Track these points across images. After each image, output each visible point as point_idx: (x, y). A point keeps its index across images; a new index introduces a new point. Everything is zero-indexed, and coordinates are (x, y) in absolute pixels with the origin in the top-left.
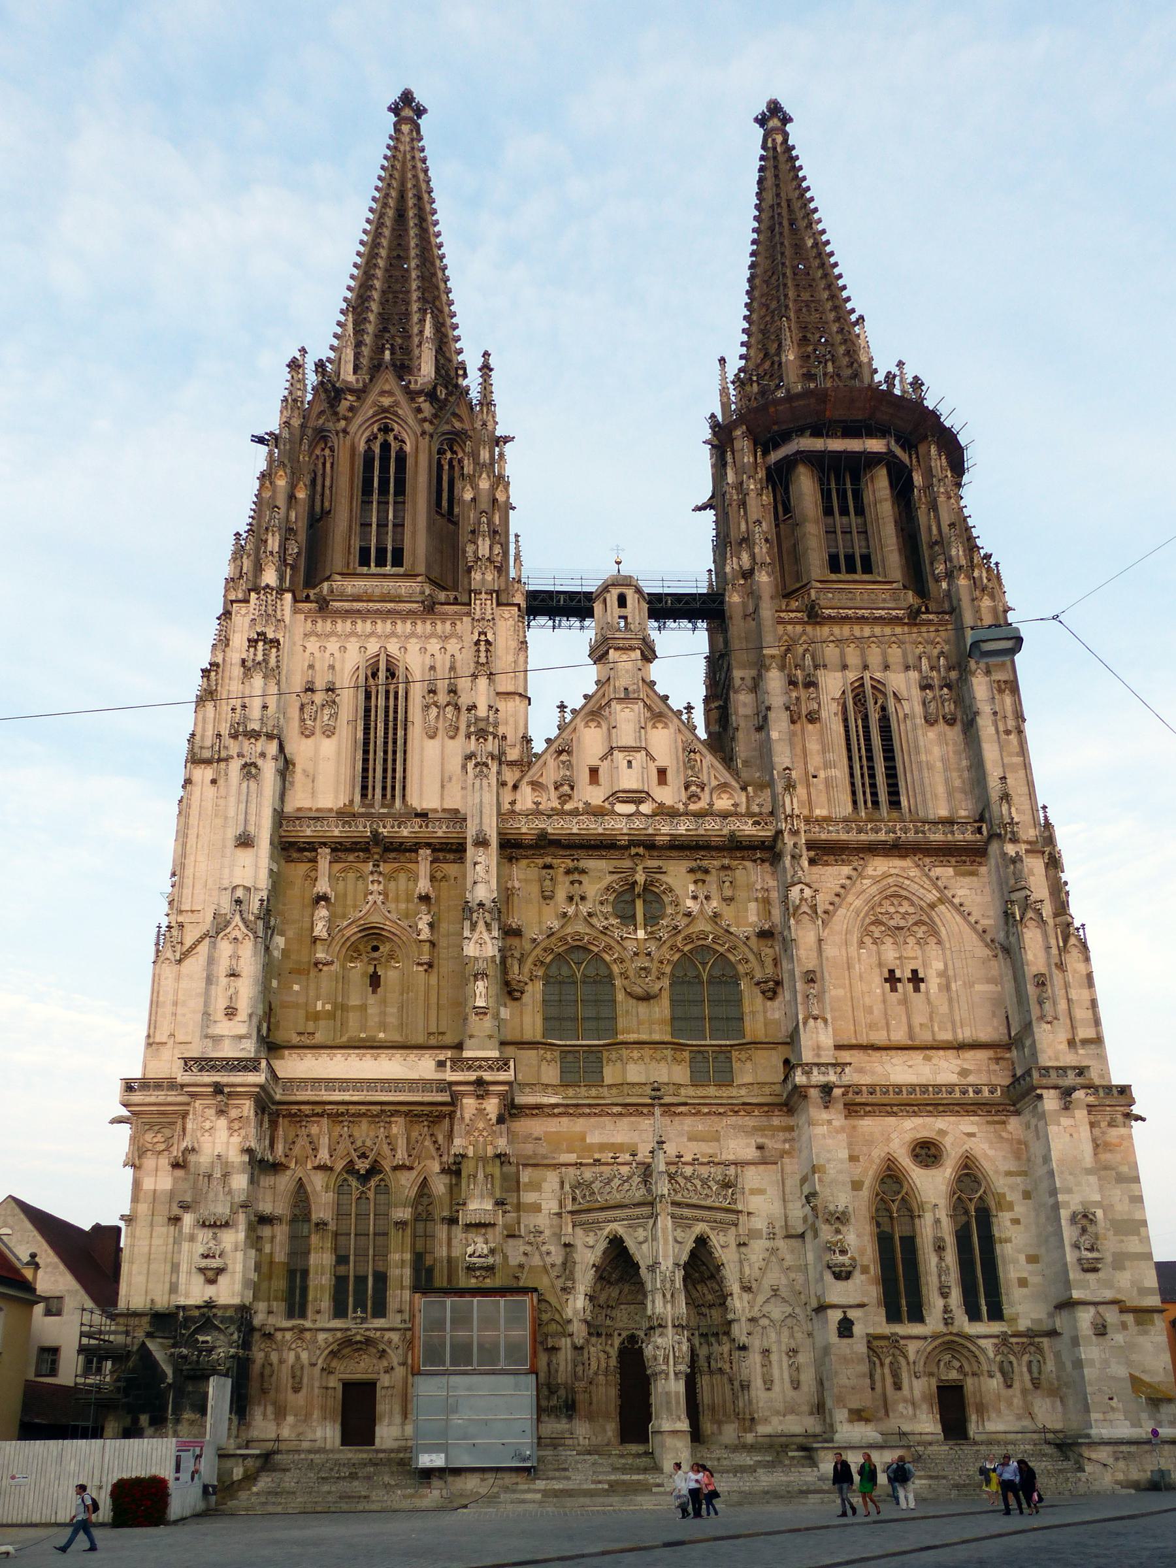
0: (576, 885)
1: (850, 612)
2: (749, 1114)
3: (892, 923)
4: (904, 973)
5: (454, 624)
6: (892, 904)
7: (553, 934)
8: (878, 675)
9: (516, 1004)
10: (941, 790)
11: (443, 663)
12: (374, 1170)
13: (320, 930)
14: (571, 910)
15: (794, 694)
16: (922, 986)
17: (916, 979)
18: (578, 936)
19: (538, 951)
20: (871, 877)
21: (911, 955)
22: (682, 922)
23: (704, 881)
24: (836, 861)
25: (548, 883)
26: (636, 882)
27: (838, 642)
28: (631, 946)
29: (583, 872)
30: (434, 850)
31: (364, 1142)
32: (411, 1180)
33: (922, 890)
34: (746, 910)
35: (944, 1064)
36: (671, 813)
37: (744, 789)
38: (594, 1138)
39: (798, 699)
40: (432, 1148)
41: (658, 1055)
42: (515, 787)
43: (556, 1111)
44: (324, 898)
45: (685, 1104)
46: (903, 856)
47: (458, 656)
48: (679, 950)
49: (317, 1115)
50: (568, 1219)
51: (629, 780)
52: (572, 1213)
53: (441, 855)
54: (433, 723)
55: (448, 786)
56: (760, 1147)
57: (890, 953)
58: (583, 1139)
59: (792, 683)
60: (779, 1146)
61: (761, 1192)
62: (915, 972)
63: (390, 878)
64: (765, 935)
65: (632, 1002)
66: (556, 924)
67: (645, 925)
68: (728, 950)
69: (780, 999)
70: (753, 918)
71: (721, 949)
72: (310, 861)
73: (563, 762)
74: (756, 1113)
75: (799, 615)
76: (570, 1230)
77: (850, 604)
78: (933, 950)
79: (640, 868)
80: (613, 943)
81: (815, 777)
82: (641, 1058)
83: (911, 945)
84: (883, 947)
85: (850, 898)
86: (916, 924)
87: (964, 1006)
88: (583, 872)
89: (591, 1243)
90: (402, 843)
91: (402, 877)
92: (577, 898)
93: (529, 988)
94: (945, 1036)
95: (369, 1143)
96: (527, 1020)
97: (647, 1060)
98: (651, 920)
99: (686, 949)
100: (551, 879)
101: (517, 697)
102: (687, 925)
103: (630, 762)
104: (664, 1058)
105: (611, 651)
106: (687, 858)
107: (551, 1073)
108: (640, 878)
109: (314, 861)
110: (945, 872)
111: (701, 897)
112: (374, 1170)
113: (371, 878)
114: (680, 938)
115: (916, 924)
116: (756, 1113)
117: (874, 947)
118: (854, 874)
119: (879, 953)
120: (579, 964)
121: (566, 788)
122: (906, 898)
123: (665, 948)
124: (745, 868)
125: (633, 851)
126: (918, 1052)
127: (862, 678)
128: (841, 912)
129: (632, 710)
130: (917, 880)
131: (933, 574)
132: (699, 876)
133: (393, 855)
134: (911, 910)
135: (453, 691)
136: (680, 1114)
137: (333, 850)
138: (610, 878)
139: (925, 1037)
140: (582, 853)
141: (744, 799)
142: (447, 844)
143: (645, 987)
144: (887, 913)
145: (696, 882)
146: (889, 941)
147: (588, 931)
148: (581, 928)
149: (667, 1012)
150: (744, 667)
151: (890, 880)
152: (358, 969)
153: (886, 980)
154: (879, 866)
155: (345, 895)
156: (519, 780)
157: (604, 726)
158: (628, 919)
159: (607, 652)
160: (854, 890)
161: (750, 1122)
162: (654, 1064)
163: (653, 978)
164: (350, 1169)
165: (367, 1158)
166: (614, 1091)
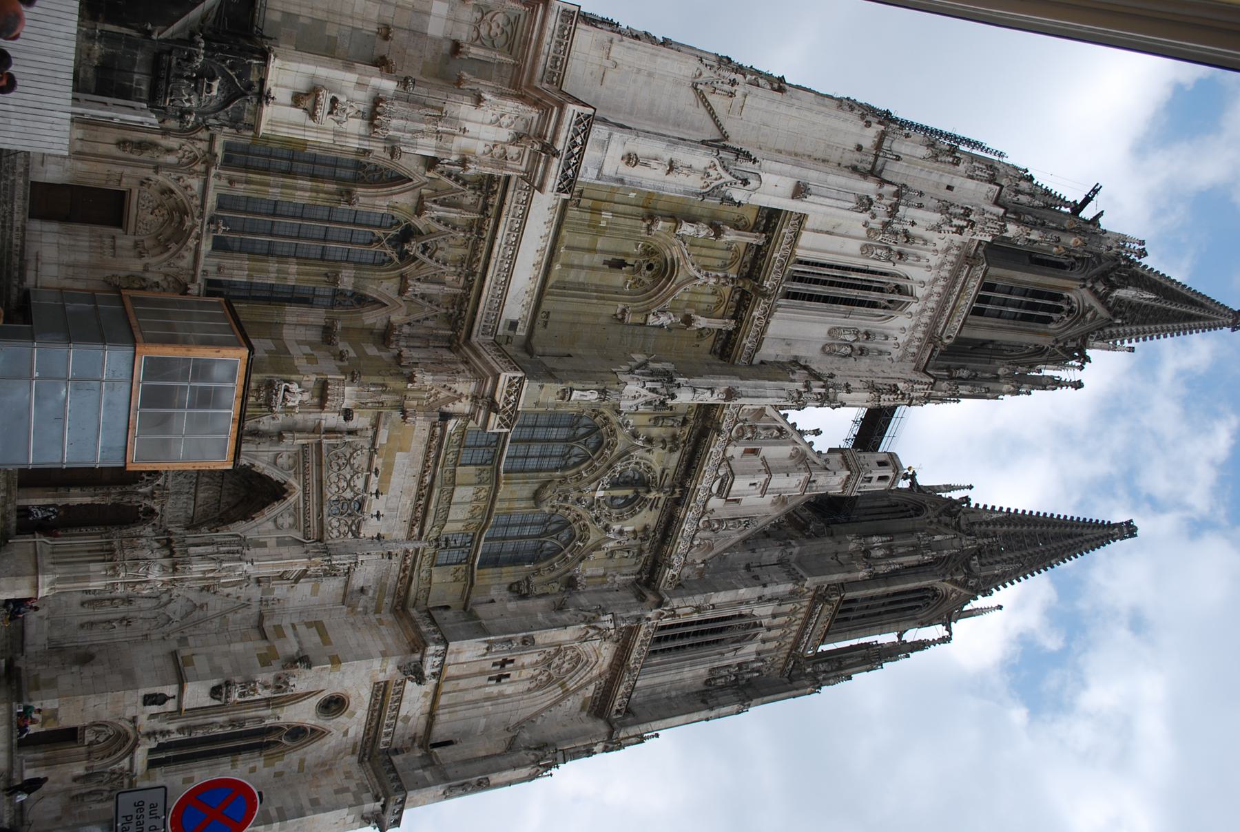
2: (400, 580)
5: (914, 354)
6: (572, 658)
8: (760, 636)
11: (889, 346)
12: (405, 257)
13: (687, 229)
20: (600, 646)
26: (649, 491)
27: (794, 612)
29: (671, 451)
30: (729, 333)
31: (442, 249)
32: (387, 292)
37: (704, 562)
38: (400, 458)
40: (420, 315)
41: (478, 511)
44: (718, 232)
46: (610, 666)
47: (887, 357)
49: (485, 207)
50: (311, 440)
51: (740, 485)
52: (319, 445)
53: (724, 337)
54: (842, 337)
55: (784, 343)
56: (362, 590)
58: (401, 450)
60: (362, 603)
61: (315, 592)
62: (508, 676)
64: (571, 584)
65: (536, 486)
68: (564, 555)
69: (508, 594)
70: (589, 572)
71: (566, 551)
72: (756, 223)
73: (771, 434)
76: (299, 441)
78: (527, 685)
80: (596, 473)
86: (549, 674)
87: (468, 714)
89: (279, 461)
90: (746, 309)
92: (650, 447)
94: (443, 700)
95: (439, 254)
97: (475, 504)
99: (575, 526)
103: (755, 484)
105: (849, 473)
108: (652, 495)
109: (755, 228)
110: (590, 691)
112: (405, 257)
113: (720, 274)
115: (549, 674)
121: (749, 435)
122: (574, 667)
124: (636, 564)
127: (761, 626)
129: (797, 486)
131: (819, 662)
133: (737, 296)
135: (863, 352)
136: (411, 530)
137: (759, 248)
138: (658, 469)
140: (688, 449)
142: (733, 345)
145: (634, 532)
147: (615, 453)
150: (800, 553)
151: (593, 659)
157: (789, 463)
159: (849, 469)
161: (391, 581)
162: (469, 507)
164: (409, 233)
165: (423, 253)
166: (448, 475)
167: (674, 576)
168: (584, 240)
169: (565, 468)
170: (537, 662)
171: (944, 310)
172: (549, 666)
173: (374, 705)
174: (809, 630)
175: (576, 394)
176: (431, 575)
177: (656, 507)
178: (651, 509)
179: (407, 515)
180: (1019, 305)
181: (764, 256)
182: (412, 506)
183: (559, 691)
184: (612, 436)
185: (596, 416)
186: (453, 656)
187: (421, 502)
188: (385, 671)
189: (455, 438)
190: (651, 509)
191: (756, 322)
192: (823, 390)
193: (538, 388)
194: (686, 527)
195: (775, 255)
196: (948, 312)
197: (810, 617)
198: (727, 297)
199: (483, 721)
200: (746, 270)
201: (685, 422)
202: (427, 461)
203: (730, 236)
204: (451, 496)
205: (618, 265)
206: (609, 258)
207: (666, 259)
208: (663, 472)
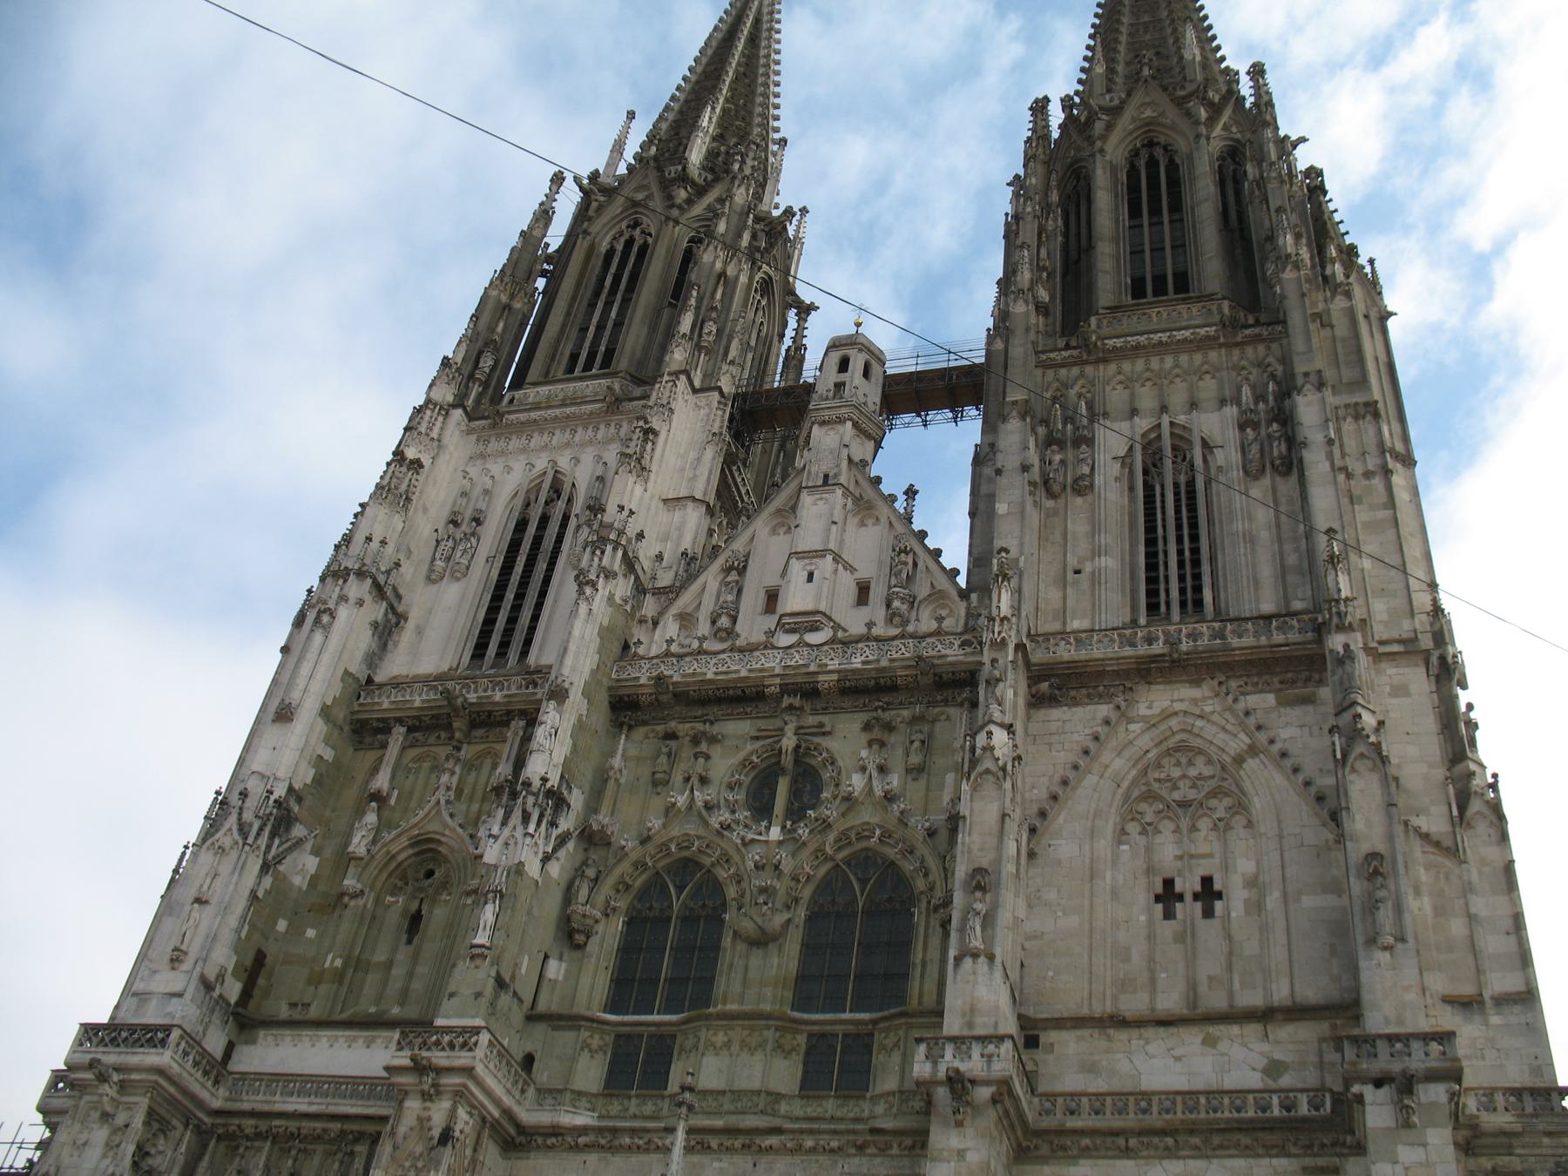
0: (701, 760)
1: (1142, 339)
2: (883, 1150)
3: (1177, 795)
4: (1188, 884)
6: (1178, 764)
7: (649, 838)
8: (1181, 419)
9: (577, 954)
10: (1266, 572)
13: (359, 844)
14: (681, 800)
15: (1057, 458)
16: (1218, 905)
17: (1208, 893)
18: (685, 842)
19: (625, 867)
20: (1144, 719)
21: (1203, 848)
22: (831, 812)
23: (882, 744)
24: (1089, 696)
25: (663, 759)
27: (1128, 383)
28: (754, 854)
33: (1222, 735)
34: (942, 786)
35: (1237, 1052)
36: (846, 643)
39: (1062, 462)
42: (655, 623)
43: (582, 1140)
44: (377, 797)
45: (777, 1131)
46: (1197, 683)
48: (827, 859)
57: (1167, 850)
59: (1050, 441)
62: (1207, 881)
63: (470, 766)
65: (741, 947)
66: (655, 823)
67: (786, 818)
73: (727, 584)
74: (895, 1151)
75: (1075, 353)
77: (1140, 328)
79: (790, 730)
80: (732, 852)
81: (1077, 572)
82: (727, 1045)
83: (1203, 833)
84: (1159, 839)
85: (1106, 757)
86: (1215, 793)
88: (713, 740)
90: (490, 713)
91: (488, 762)
93: (600, 928)
94: (1251, 998)
96: (585, 980)
97: (735, 1047)
98: (796, 813)
99: (841, 856)
100: (669, 755)
101: (690, 505)
102: (843, 815)
104: (762, 1045)
106: (864, 708)
107: (590, 1073)
109: (384, 746)
110: (1263, 701)
111: (872, 768)
114: (831, 837)
116: (895, 1151)
117: (1141, 841)
118: (1113, 716)
119: (1149, 850)
120: (680, 889)
121: (724, 621)
122: (1200, 752)
123: (805, 854)
125: (786, 701)
126: (1195, 1030)
128: (1090, 780)
130: (1215, 718)
132: (876, 733)
133: (479, 732)
134: (1208, 771)
137: (410, 730)
138: (750, 747)
139: (1215, 1000)
140: (714, 711)
141: (963, 613)
143: (759, 920)
144: (1169, 779)
145: (870, 744)
146: (1167, 827)
147: (701, 832)
148: (692, 828)
149: (793, 966)
152: (398, 904)
153: (1158, 899)
154: (1157, 699)
155: (411, 793)
156: (661, 614)
158: (762, 809)
160: (1113, 743)
162: (745, 1055)
163: (779, 905)
167: (964, 644)
168: (372, 980)
169: (724, 906)
170: (1177, 830)
171: (568, 417)
172: (1185, 804)
173: (1196, 1148)
174: (1164, 337)
175: (481, 939)
176: (881, 1096)
177: (821, 725)
178: (829, 733)
179: (743, 1162)
180: (609, 304)
181: (417, 718)
182: (726, 1158)
183: (1251, 764)
184: (669, 849)
185: (628, 887)
186: (978, 1020)
187: (714, 1144)
188: (961, 1154)
189: (615, 1108)
190: (829, 733)
191: (514, 691)
192: (588, 549)
193: (453, 1000)
194: (857, 662)
195: (417, 704)
196: (568, 410)
197: (1137, 347)
198: (483, 746)
199: (1308, 901)
200: (443, 735)
201: (671, 736)
202: (639, 1147)
203: (382, 781)
204: (711, 1092)
205: (415, 922)
206: (405, 937)
207: (415, 855)
208: (757, 738)
